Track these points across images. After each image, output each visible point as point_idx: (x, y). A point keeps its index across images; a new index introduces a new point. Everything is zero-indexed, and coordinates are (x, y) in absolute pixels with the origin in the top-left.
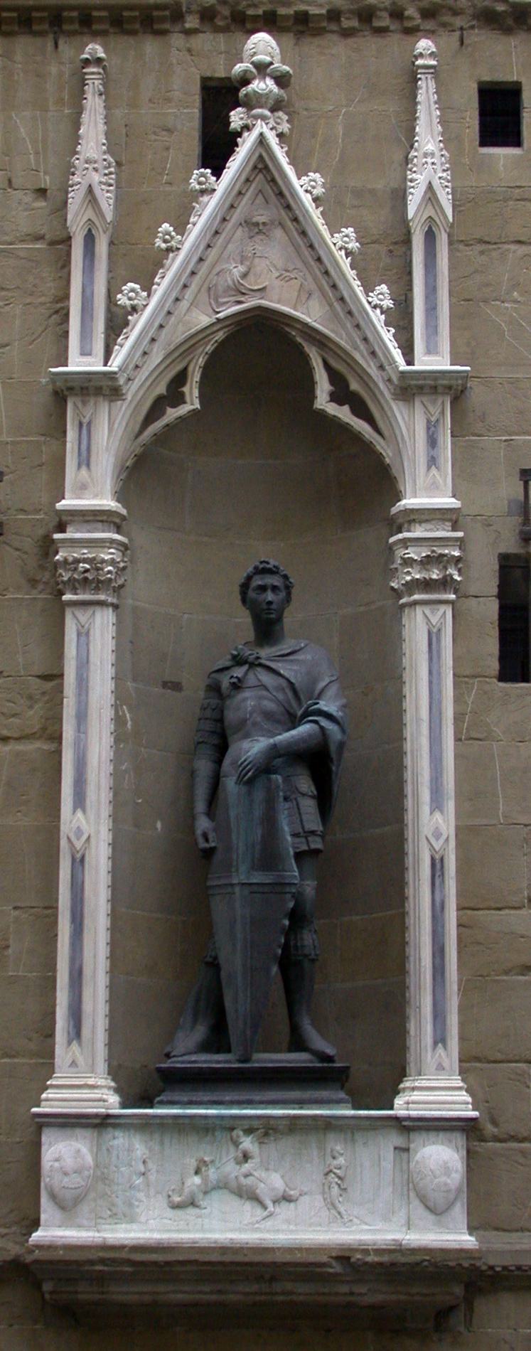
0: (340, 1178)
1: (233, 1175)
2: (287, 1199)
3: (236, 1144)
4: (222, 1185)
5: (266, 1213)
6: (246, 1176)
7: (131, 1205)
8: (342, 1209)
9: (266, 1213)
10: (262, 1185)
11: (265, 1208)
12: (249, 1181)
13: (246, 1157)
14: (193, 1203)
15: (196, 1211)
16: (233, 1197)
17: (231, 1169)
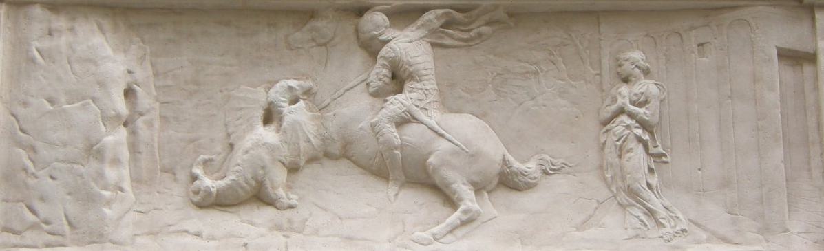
0: (644, 125)
1: (365, 124)
2: (509, 182)
3: (371, 48)
4: (337, 151)
5: (455, 217)
6: (403, 121)
7: (89, 199)
8: (656, 203)
9: (455, 217)
10: (443, 145)
11: (449, 200)
12: (413, 133)
13: (398, 78)
14: (259, 196)
15: (269, 212)
16: (372, 181)
17: (359, 111)
